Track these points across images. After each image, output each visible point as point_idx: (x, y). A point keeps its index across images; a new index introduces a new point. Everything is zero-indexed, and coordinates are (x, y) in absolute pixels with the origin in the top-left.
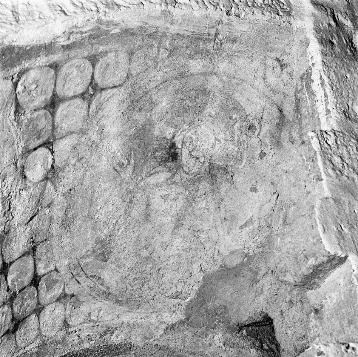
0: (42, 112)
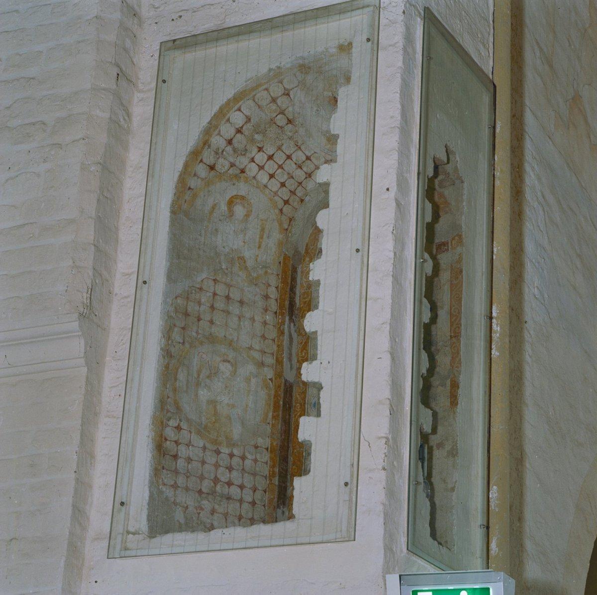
0: (271, 104)
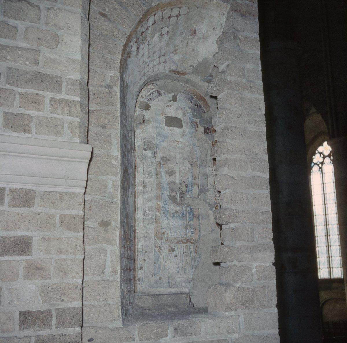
0: (167, 19)
